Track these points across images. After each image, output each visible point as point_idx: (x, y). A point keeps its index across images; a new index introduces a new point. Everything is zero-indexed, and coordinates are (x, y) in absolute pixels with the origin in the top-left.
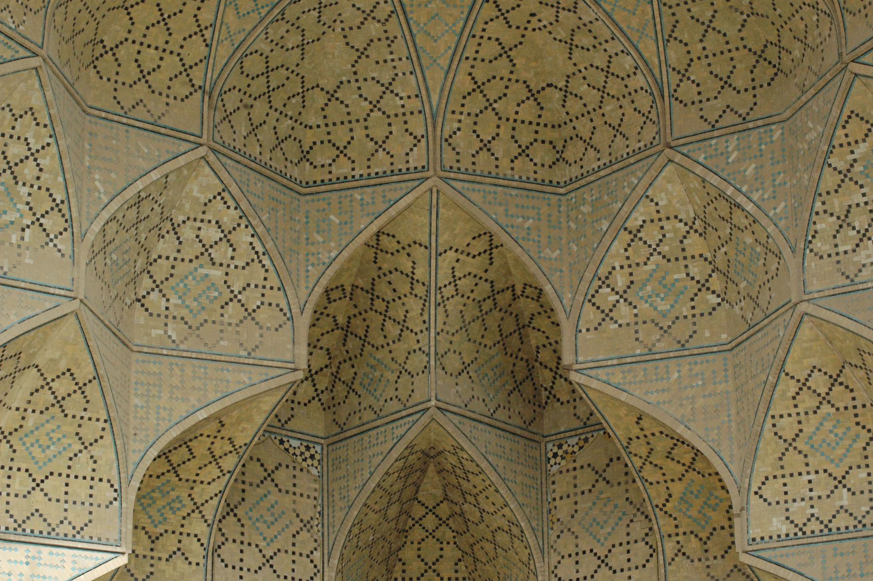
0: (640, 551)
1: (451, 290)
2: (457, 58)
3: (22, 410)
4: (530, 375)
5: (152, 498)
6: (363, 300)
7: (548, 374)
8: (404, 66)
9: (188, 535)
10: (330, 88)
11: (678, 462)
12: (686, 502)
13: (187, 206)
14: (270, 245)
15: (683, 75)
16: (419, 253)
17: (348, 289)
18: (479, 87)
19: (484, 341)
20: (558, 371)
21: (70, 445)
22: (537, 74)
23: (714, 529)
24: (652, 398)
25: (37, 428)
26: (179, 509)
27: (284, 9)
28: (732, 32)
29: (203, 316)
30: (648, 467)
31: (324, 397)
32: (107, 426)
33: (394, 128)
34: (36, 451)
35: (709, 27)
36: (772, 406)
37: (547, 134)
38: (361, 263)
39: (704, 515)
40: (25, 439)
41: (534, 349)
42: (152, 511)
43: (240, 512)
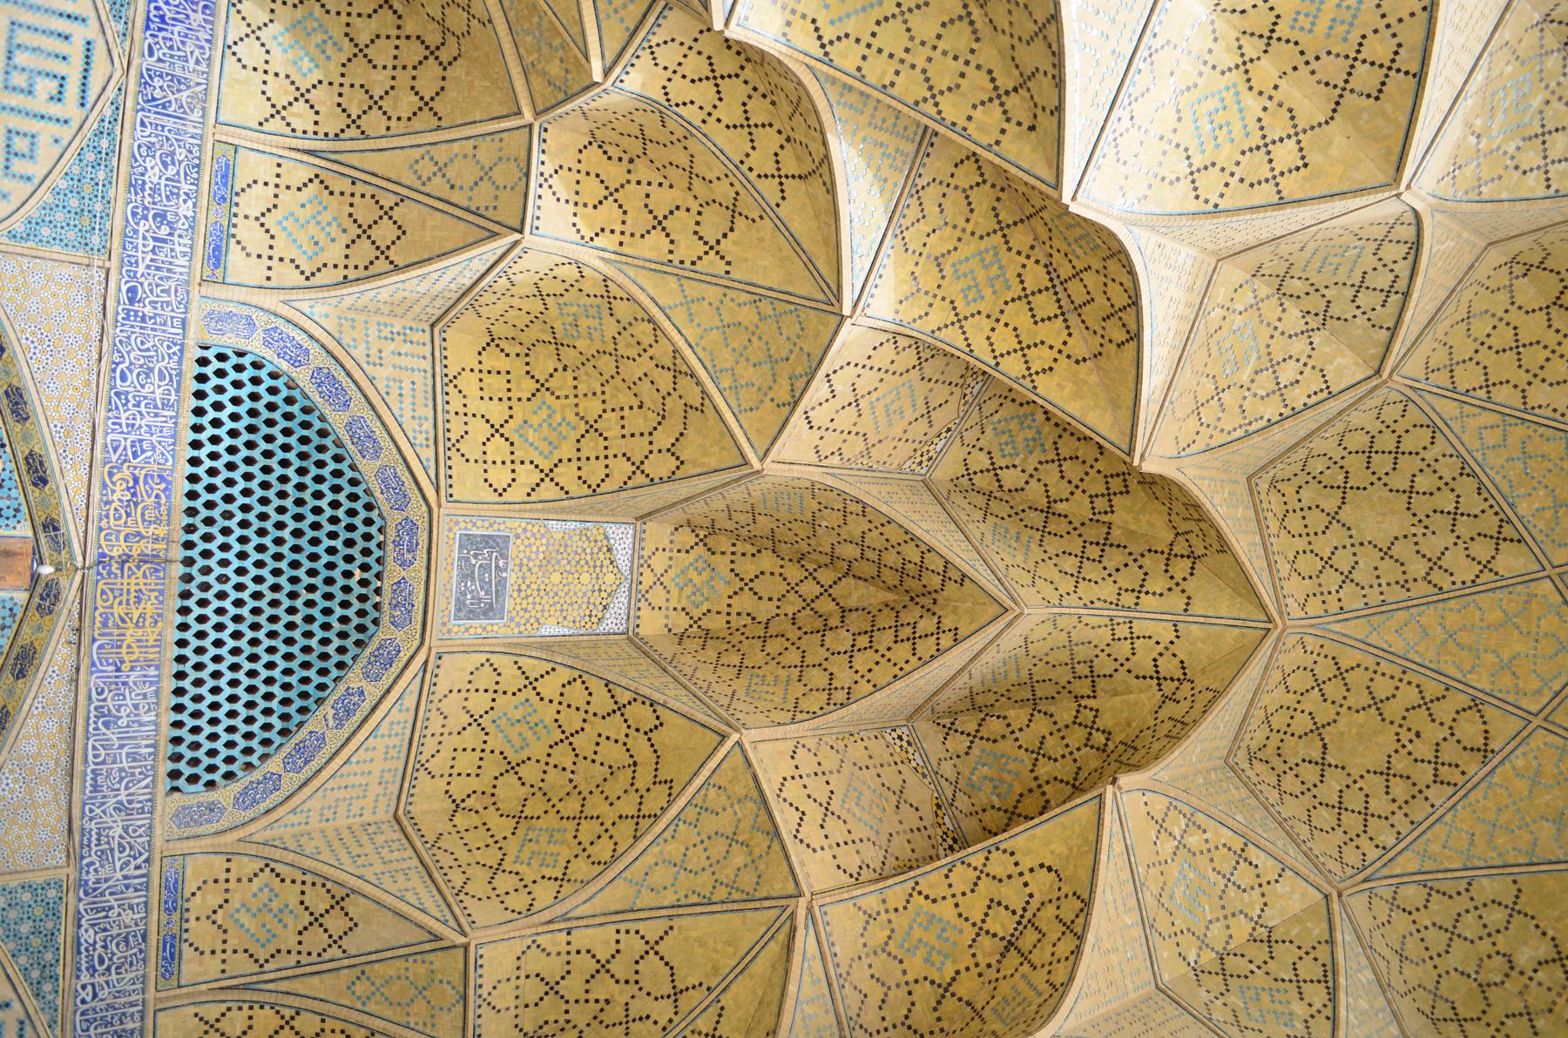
0: (852, 862)
1: (1123, 631)
2: (1381, 653)
3: (1273, 93)
4: (975, 707)
5: (992, 264)
7: (971, 727)
8: (1374, 597)
9: (931, 305)
10: (1342, 516)
11: (986, 915)
13: (1327, 350)
14: (1256, 439)
17: (1106, 518)
18: (1341, 674)
22: (1342, 734)
26: (966, 297)
27: (1475, 475)
29: (1214, 352)
30: (973, 875)
31: (965, 481)
32: (1210, 207)
33: (1307, 581)
34: (1213, 104)
35: (1453, 933)
37: (1273, 744)
38: (1143, 535)
39: (917, 947)
40: (1232, 91)
42: (974, 263)
43: (915, 373)
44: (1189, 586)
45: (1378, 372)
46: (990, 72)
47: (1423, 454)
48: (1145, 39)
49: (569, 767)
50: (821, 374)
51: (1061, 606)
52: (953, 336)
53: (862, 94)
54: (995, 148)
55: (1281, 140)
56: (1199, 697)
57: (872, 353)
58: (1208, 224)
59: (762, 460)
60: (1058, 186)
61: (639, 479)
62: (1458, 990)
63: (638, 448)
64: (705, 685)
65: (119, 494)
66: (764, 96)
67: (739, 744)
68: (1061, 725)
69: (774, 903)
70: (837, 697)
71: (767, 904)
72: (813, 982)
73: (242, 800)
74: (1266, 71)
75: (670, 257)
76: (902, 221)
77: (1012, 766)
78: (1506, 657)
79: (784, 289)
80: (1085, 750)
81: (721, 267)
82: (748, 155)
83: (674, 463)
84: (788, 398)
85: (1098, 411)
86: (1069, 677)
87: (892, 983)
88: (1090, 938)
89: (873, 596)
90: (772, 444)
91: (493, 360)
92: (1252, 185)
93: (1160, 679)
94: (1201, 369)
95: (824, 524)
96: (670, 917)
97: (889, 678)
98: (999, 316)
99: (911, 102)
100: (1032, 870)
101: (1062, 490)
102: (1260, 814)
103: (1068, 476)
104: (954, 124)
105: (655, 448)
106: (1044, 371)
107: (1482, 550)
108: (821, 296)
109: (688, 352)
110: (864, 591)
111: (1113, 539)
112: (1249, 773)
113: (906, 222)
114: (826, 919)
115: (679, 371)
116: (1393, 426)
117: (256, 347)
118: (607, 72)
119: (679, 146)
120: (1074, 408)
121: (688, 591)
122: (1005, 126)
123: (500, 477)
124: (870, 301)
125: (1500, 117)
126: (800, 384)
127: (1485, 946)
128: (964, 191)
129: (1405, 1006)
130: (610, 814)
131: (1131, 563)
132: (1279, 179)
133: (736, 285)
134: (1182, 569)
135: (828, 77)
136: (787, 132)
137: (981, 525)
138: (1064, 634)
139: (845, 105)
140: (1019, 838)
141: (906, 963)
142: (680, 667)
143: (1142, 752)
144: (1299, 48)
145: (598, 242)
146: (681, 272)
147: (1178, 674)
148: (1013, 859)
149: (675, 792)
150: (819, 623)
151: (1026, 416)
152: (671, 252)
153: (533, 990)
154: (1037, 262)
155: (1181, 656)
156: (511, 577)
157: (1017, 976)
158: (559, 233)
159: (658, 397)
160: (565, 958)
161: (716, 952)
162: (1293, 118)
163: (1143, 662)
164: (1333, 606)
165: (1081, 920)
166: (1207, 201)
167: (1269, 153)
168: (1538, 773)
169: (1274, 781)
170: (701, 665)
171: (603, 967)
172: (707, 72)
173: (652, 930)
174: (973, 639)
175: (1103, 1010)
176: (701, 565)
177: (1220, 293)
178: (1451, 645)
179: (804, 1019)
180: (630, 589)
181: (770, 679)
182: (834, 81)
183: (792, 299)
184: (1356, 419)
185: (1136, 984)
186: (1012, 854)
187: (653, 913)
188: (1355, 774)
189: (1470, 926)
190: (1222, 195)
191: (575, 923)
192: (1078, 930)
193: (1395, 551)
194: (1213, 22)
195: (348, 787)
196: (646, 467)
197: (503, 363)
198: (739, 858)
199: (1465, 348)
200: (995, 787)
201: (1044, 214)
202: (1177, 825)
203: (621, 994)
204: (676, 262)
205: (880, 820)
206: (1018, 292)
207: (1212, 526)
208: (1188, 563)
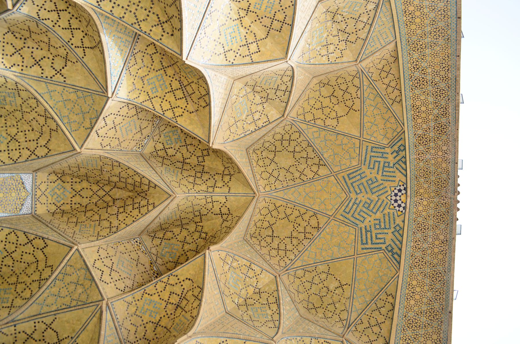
0: (121, 286)
3: (249, 28)
4: (162, 229)
5: (160, 80)
7: (161, 236)
8: (285, 184)
9: (140, 94)
10: (275, 160)
11: (169, 297)
12: (150, 302)
13: (268, 109)
14: (248, 137)
16: (226, 189)
17: (202, 164)
19: (183, 213)
21: (228, 45)
23: (141, 317)
24: (209, 285)
25: (239, 33)
26: (152, 91)
28: (313, 291)
30: (164, 285)
31: (155, 153)
32: (231, 63)
33: (265, 181)
34: (230, 30)
35: (312, 283)
36: (230, 339)
38: (214, 169)
39: (146, 312)
40: (237, 26)
41: (171, 230)
42: (154, 80)
44: (229, 184)
45: (283, 116)
46: (157, 15)
47: (297, 140)
48: (209, 8)
49: (11, 264)
50: (101, 117)
51: (189, 193)
52: (148, 104)
53: (113, 20)
54: (160, 41)
55: (252, 43)
56: (234, 219)
57: (120, 110)
58: (230, 69)
59: (81, 148)
60: (181, 54)
61: (33, 157)
62: (315, 299)
63: (32, 145)
64: (63, 230)
66: (76, 18)
67: (77, 250)
68: (191, 232)
69: (94, 304)
70: (113, 230)
71: (91, 304)
72: (110, 329)
74: (247, 21)
75: (42, 75)
76: (129, 65)
77: (175, 247)
78: (323, 200)
79: (86, 87)
80: (199, 240)
81: (62, 79)
82: (71, 39)
83: (46, 150)
84: (90, 126)
85: (198, 129)
86: (193, 216)
87: (139, 325)
88: (204, 300)
89: (125, 194)
90: (84, 142)
92: (243, 57)
93: (222, 214)
94: (230, 115)
95: (105, 170)
96: (55, 315)
97: (131, 222)
98: (164, 97)
99: (130, 24)
100: (183, 281)
101: (187, 155)
102: (254, 254)
103: (190, 150)
104: (145, 32)
105: (39, 145)
106: (180, 116)
108: (101, 90)
109: (50, 110)
110: (121, 192)
111: (205, 170)
112: (251, 241)
113: (130, 65)
114: (113, 307)
115: (47, 116)
116: (288, 132)
118: (14, 6)
119: (44, 35)
120: (190, 128)
121: (55, 197)
122: (163, 34)
124: (118, 92)
125: (315, 39)
126: (94, 121)
127: (321, 285)
128: (150, 55)
129: (300, 306)
130: (28, 280)
131: (211, 178)
132: (252, 55)
133: (68, 86)
134: (227, 179)
135: (100, 13)
136: (86, 31)
137: (161, 168)
138: (190, 203)
139: (107, 23)
140: (179, 271)
141: (143, 317)
142: (53, 224)
143: (217, 238)
144: (257, 14)
145: (12, 69)
146: (46, 81)
147: (228, 212)
148: (177, 278)
149: (54, 269)
150: (105, 205)
151: (174, 131)
152: (42, 73)
154: (176, 80)
155: (228, 207)
157: (181, 316)
159: (39, 127)
160: (14, 335)
161: (74, 324)
162: (255, 36)
163: (216, 209)
165: (200, 294)
166: (230, 61)
167: (248, 47)
168: (333, 233)
169: (258, 243)
170: (61, 223)
172: (54, 8)
173: (48, 320)
174: (160, 206)
175: (209, 322)
176: (59, 187)
177: (235, 91)
178: (307, 197)
179: (108, 342)
180: (32, 198)
181: (88, 226)
182: (102, 15)
183: (89, 91)
184: (278, 130)
185: (219, 312)
186: (177, 276)
187: (48, 314)
188: (282, 238)
189: (317, 280)
190: (234, 60)
191: (17, 322)
192: (200, 298)
193: (290, 170)
194: (230, 4)
196: (36, 152)
198: (80, 290)
199: (308, 108)
200: (170, 255)
201: (178, 64)
202: (229, 260)
204: (44, 77)
205: (131, 270)
206: (169, 89)
207: (236, 165)
208: (229, 177)
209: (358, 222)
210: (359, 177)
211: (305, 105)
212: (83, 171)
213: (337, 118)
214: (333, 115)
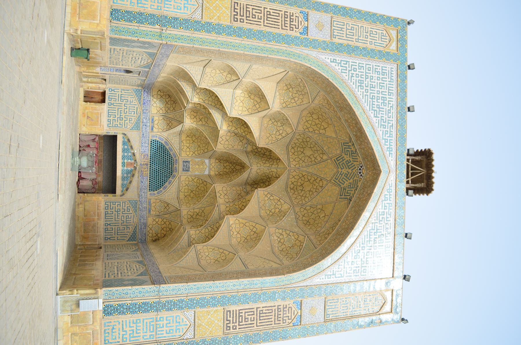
0: (227, 200)
4: (256, 184)
6: (269, 157)
8: (307, 164)
15: (305, 209)
18: (303, 176)
20: (256, 188)
28: (312, 217)
35: (313, 213)
37: (295, 187)
65: (143, 157)
73: (158, 193)
91: (188, 138)
107: (321, 156)
117: (157, 139)
123: (188, 153)
127: (317, 215)
153: (189, 217)
156: (191, 166)
158: (189, 123)
163: (274, 175)
164: (301, 165)
171: (198, 214)
173: (203, 209)
195: (171, 192)
197: (189, 139)
203: (199, 217)
209: (341, 184)
210: (341, 160)
211: (306, 124)
212: (225, 159)
213: (325, 129)
214: (322, 127)
